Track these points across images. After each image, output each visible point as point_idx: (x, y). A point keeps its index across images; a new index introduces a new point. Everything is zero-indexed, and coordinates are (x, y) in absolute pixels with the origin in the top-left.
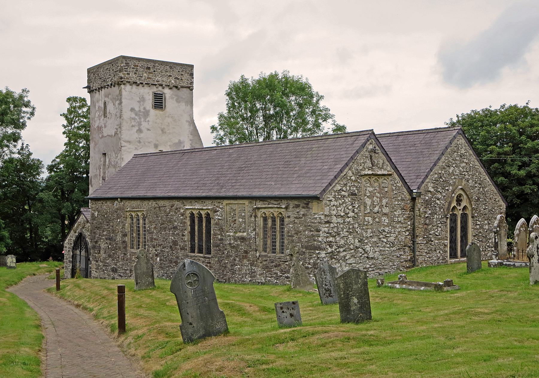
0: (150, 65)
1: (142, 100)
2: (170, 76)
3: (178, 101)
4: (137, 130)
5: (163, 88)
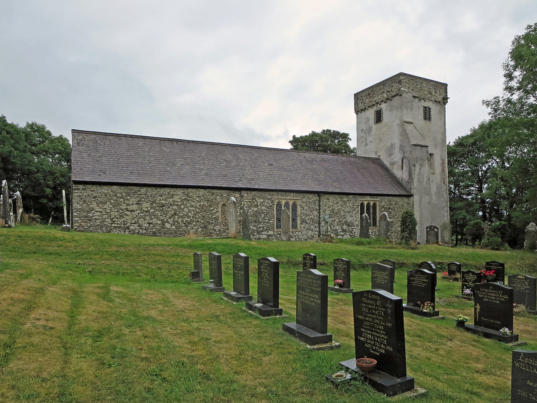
0: (370, 92)
1: (368, 120)
2: (384, 92)
3: (391, 110)
4: (365, 145)
5: (380, 105)
